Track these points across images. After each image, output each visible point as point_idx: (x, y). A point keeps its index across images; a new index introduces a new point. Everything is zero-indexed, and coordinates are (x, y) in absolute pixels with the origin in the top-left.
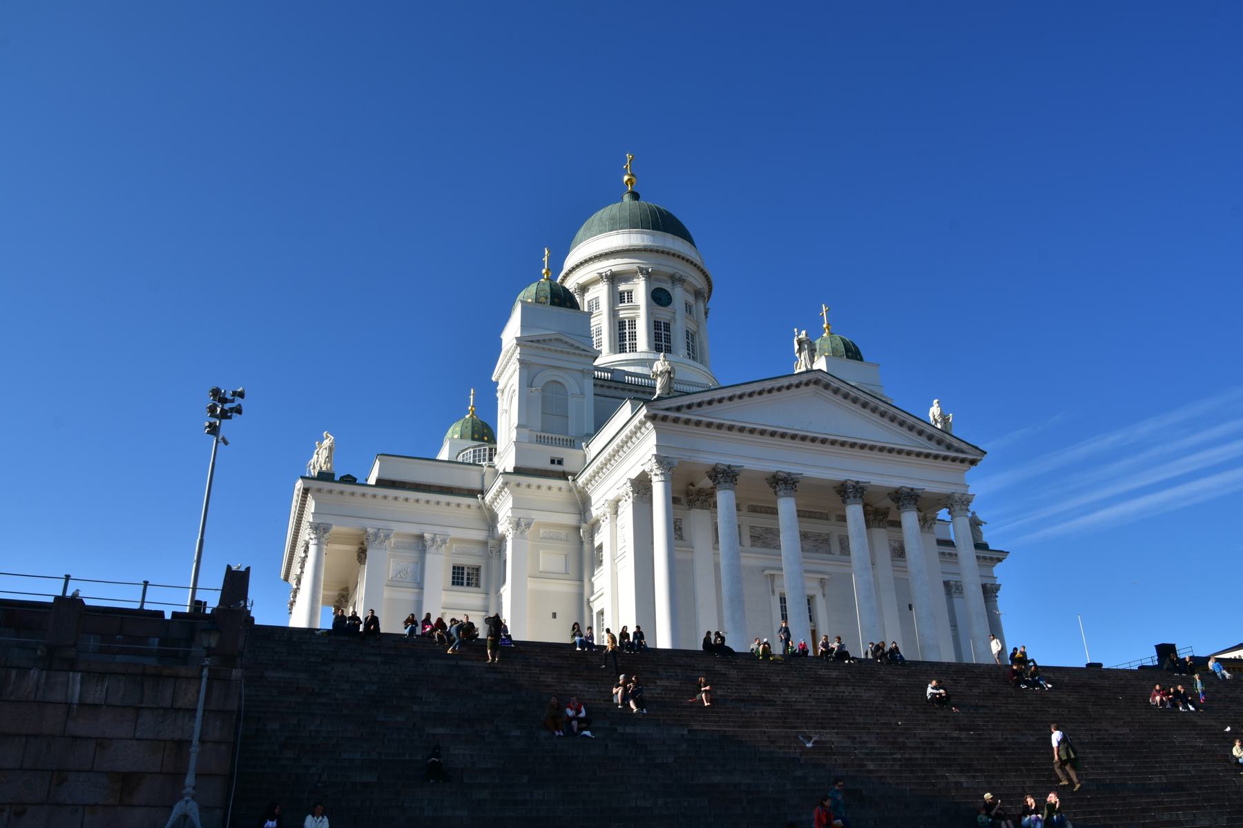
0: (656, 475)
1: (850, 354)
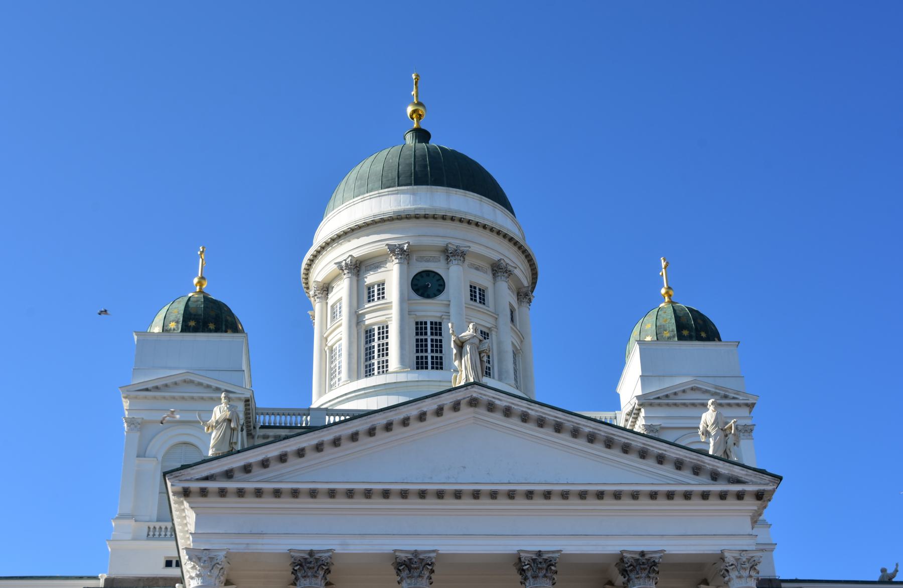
0: (192, 578)
1: (685, 333)
